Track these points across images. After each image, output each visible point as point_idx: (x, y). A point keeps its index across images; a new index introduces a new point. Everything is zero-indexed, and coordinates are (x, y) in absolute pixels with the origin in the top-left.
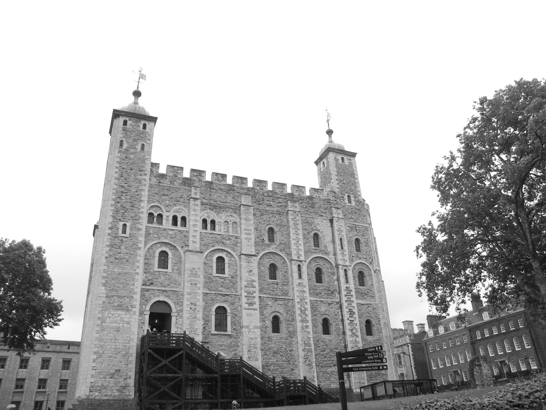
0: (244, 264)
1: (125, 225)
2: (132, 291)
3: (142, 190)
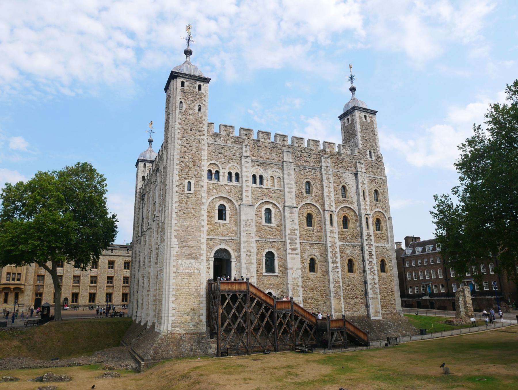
0: (287, 215)
1: (189, 183)
2: (199, 242)
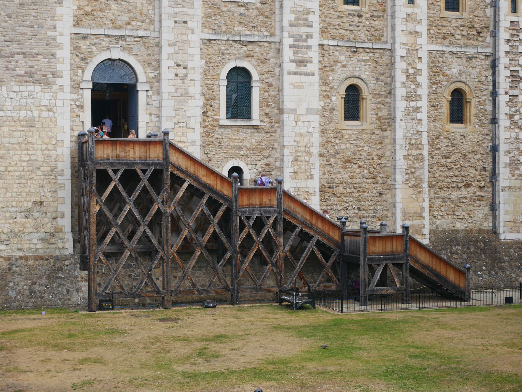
2: (51, 42)
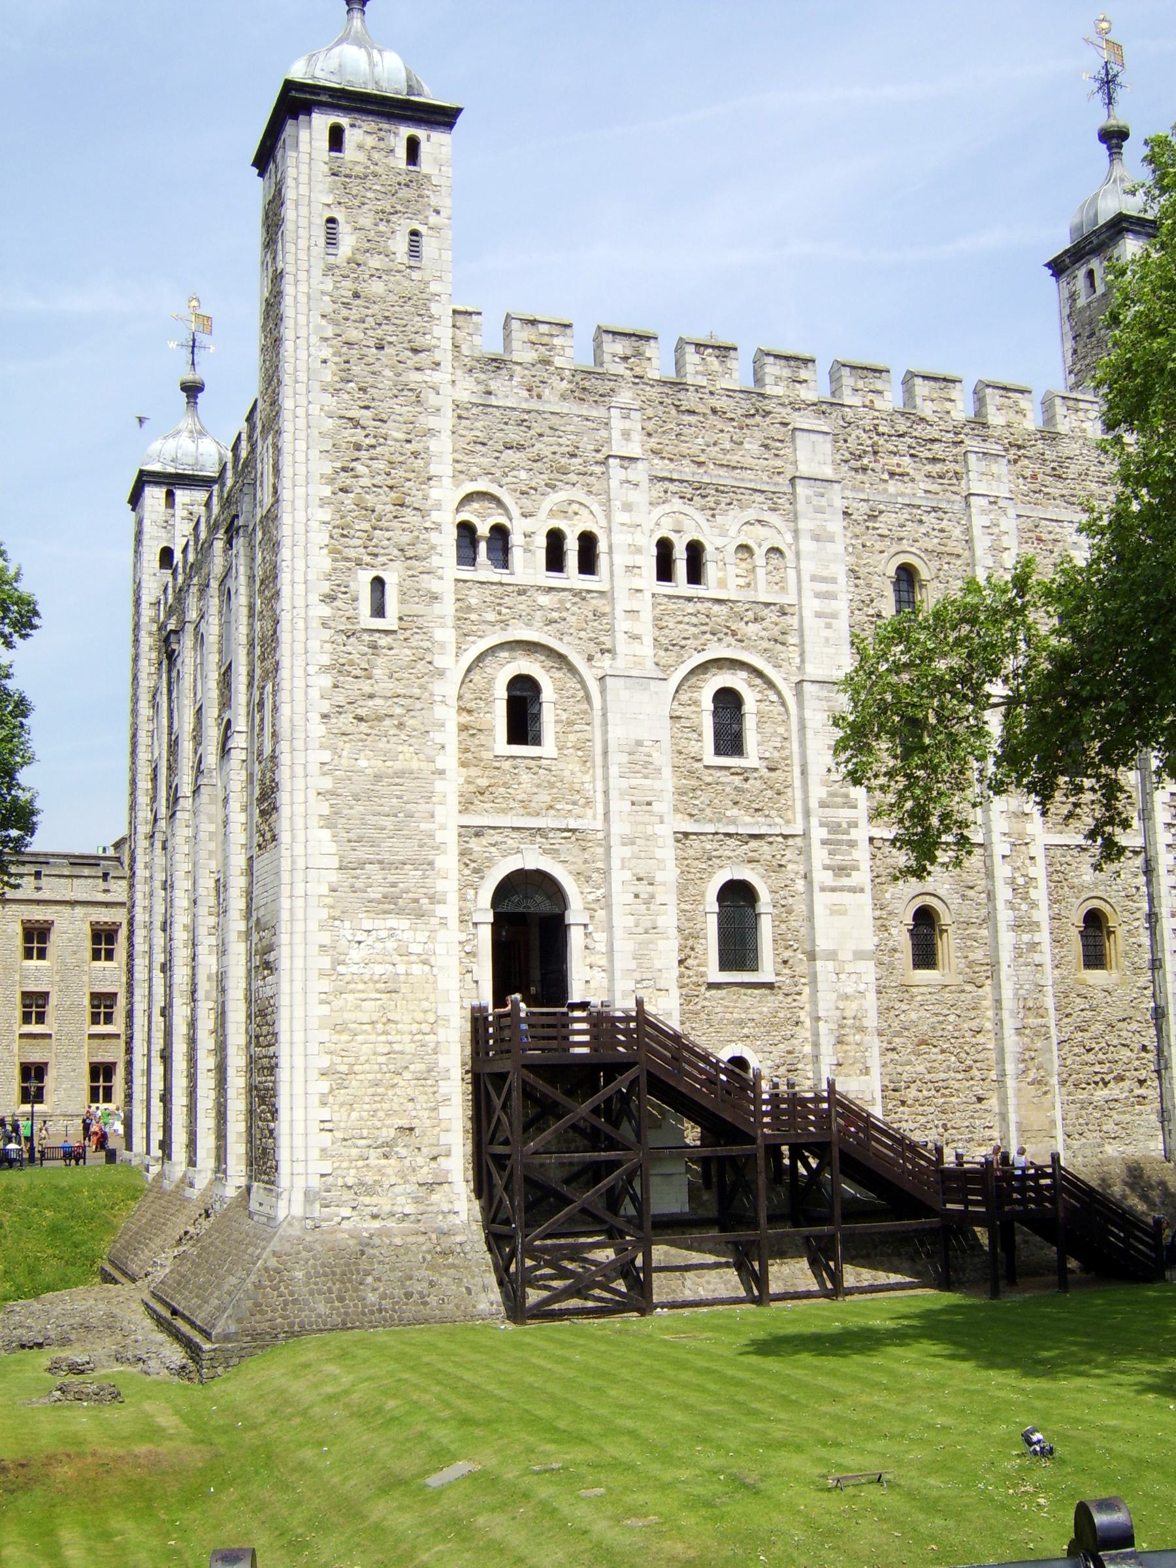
1: (378, 584)
2: (428, 842)
3: (430, 432)
